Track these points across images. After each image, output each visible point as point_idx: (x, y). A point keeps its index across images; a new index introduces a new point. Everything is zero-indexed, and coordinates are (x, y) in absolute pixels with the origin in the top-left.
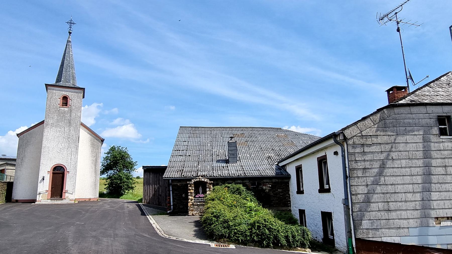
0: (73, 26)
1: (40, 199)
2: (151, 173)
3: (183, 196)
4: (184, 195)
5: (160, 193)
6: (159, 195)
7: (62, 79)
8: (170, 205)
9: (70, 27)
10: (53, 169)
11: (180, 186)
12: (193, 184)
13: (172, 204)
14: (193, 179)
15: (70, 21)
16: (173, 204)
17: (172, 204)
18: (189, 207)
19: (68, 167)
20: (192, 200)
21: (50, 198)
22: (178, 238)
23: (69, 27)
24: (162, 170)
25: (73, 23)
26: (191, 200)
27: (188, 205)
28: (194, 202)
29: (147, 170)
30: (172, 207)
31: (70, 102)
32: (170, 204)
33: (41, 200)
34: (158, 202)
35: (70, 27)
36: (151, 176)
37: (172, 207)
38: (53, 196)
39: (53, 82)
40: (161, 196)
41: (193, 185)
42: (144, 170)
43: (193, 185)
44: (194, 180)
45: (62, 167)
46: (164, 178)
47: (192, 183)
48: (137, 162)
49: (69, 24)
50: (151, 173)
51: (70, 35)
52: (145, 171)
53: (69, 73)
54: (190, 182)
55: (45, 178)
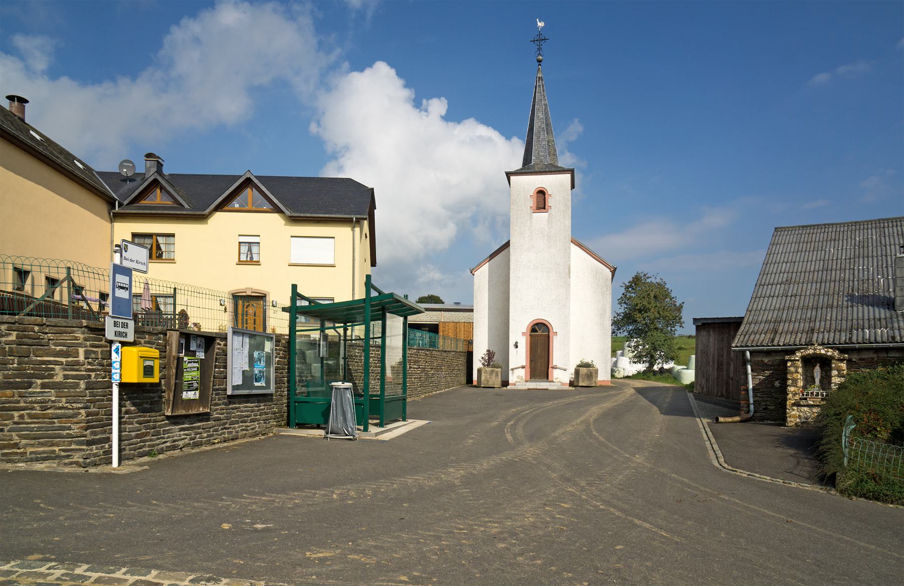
0: (544, 45)
1: (514, 382)
2: (711, 332)
3: (775, 385)
4: (779, 383)
5: (732, 375)
6: (728, 377)
7: (533, 158)
8: (747, 402)
9: (539, 49)
10: (533, 324)
11: (770, 363)
12: (798, 360)
13: (751, 401)
14: (799, 349)
15: (538, 37)
16: (754, 401)
17: (751, 401)
18: (789, 410)
19: (555, 326)
20: (796, 394)
21: (529, 379)
22: (752, 474)
23: (537, 50)
24: (731, 325)
25: (544, 38)
26: (794, 395)
27: (786, 405)
28: (801, 399)
29: (703, 325)
30: (752, 407)
31: (550, 202)
32: (749, 401)
33: (516, 382)
34: (726, 391)
35: (539, 49)
36: (711, 339)
37: (752, 407)
38: (534, 376)
39: (518, 164)
40: (732, 380)
41: (799, 363)
42: (696, 326)
43: (799, 363)
44: (802, 353)
45: (544, 325)
46: (733, 347)
47: (797, 358)
48: (683, 303)
49: (536, 42)
50: (711, 332)
51: (540, 65)
52: (698, 328)
53: (543, 143)
54: (791, 357)
55: (518, 345)
